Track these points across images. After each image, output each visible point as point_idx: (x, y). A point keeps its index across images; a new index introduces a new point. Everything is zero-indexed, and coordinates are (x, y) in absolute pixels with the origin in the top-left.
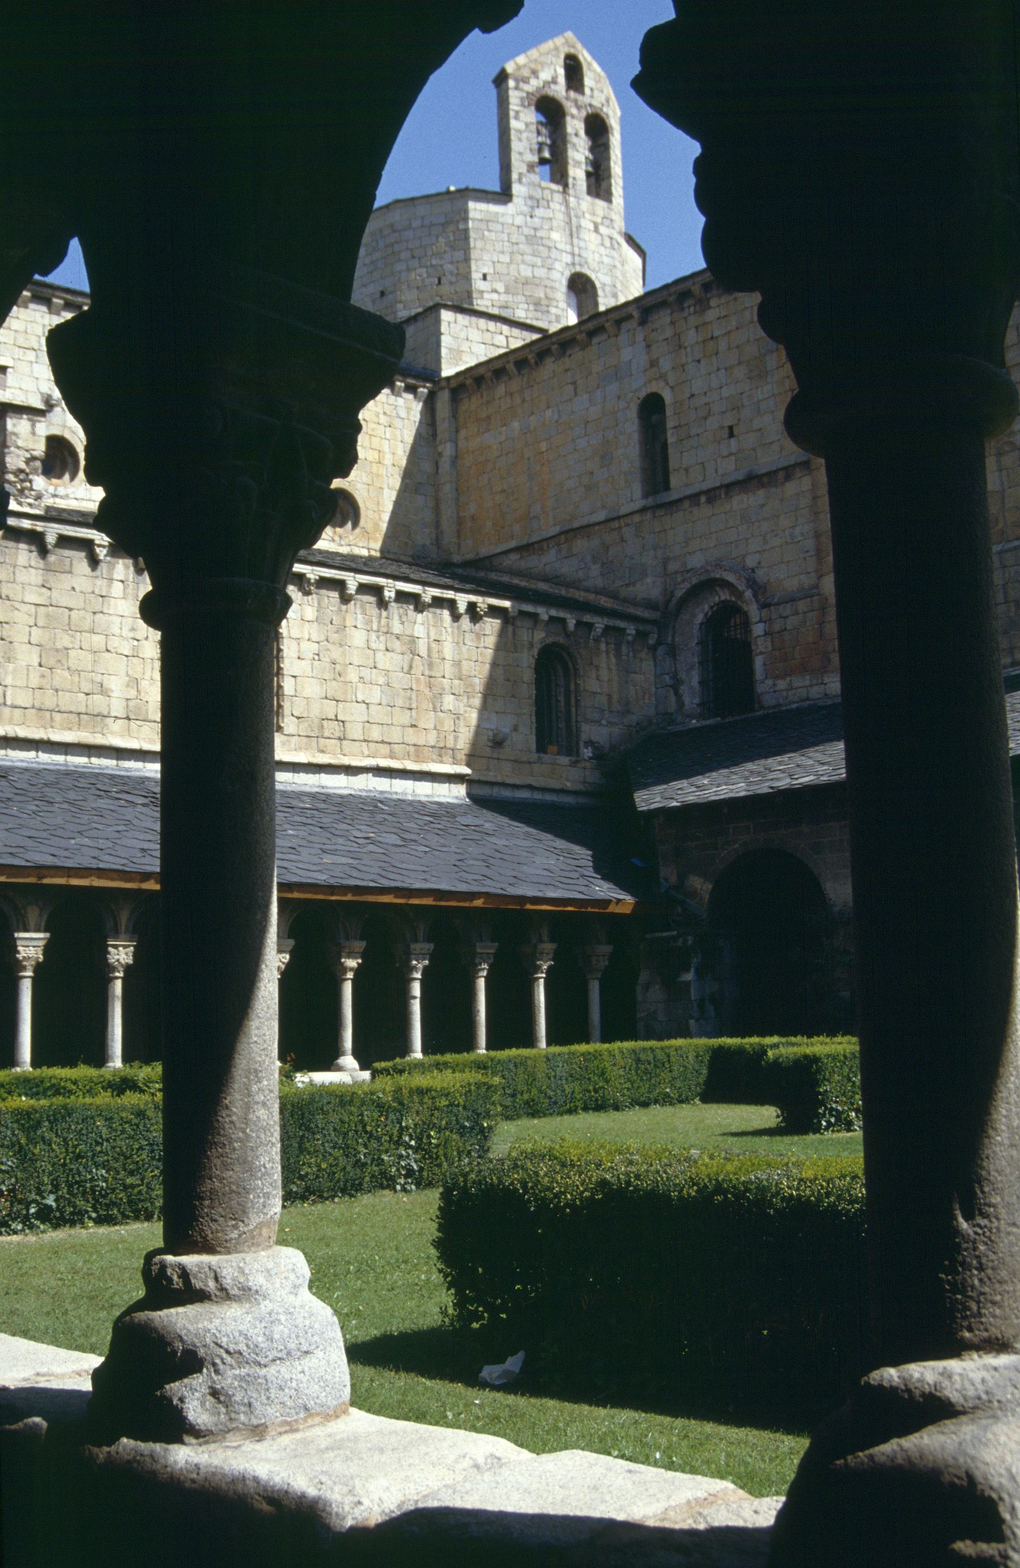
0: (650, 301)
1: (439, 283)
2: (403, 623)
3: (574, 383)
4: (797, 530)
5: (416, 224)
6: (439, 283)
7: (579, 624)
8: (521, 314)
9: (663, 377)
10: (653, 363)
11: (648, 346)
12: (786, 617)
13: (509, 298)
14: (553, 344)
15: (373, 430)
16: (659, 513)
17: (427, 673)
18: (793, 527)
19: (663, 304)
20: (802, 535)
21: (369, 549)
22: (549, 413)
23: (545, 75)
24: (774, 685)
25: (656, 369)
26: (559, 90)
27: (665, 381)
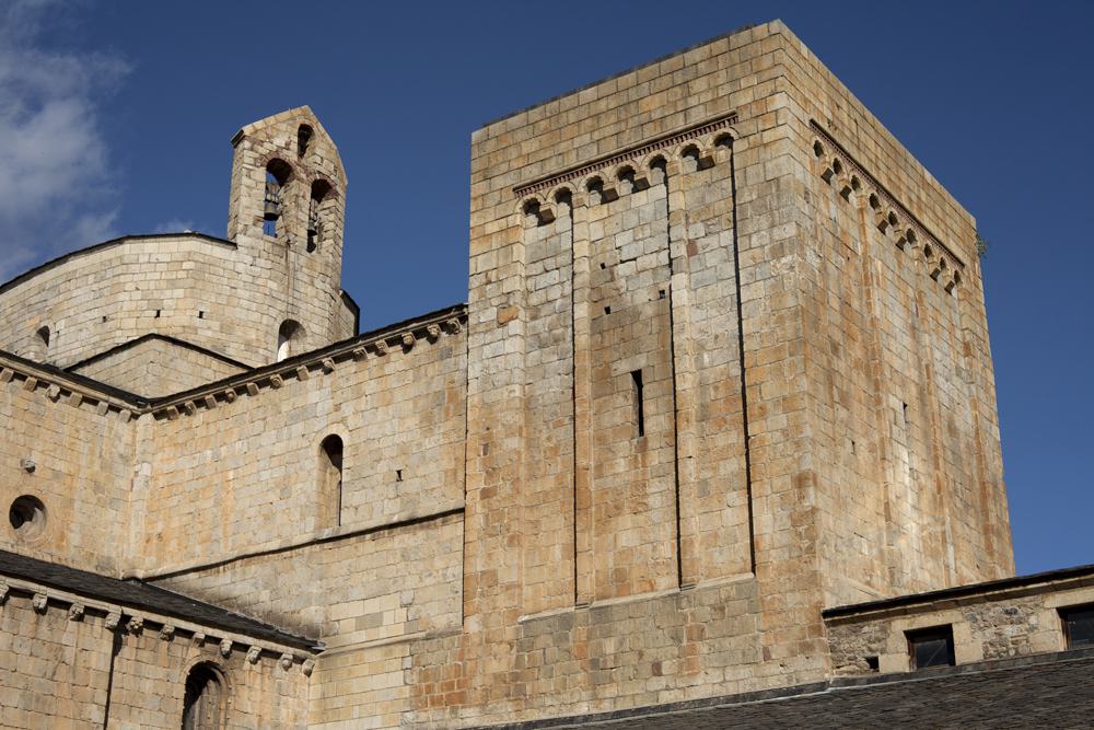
1: (158, 315)
2: (51, 630)
5: (146, 259)
6: (158, 315)
7: (236, 646)
8: (232, 352)
9: (343, 421)
10: (337, 407)
12: (433, 652)
13: (224, 337)
14: (250, 381)
16: (326, 546)
17: (71, 681)
20: (454, 576)
23: (280, 141)
24: (417, 717)
25: (338, 413)
26: (291, 156)
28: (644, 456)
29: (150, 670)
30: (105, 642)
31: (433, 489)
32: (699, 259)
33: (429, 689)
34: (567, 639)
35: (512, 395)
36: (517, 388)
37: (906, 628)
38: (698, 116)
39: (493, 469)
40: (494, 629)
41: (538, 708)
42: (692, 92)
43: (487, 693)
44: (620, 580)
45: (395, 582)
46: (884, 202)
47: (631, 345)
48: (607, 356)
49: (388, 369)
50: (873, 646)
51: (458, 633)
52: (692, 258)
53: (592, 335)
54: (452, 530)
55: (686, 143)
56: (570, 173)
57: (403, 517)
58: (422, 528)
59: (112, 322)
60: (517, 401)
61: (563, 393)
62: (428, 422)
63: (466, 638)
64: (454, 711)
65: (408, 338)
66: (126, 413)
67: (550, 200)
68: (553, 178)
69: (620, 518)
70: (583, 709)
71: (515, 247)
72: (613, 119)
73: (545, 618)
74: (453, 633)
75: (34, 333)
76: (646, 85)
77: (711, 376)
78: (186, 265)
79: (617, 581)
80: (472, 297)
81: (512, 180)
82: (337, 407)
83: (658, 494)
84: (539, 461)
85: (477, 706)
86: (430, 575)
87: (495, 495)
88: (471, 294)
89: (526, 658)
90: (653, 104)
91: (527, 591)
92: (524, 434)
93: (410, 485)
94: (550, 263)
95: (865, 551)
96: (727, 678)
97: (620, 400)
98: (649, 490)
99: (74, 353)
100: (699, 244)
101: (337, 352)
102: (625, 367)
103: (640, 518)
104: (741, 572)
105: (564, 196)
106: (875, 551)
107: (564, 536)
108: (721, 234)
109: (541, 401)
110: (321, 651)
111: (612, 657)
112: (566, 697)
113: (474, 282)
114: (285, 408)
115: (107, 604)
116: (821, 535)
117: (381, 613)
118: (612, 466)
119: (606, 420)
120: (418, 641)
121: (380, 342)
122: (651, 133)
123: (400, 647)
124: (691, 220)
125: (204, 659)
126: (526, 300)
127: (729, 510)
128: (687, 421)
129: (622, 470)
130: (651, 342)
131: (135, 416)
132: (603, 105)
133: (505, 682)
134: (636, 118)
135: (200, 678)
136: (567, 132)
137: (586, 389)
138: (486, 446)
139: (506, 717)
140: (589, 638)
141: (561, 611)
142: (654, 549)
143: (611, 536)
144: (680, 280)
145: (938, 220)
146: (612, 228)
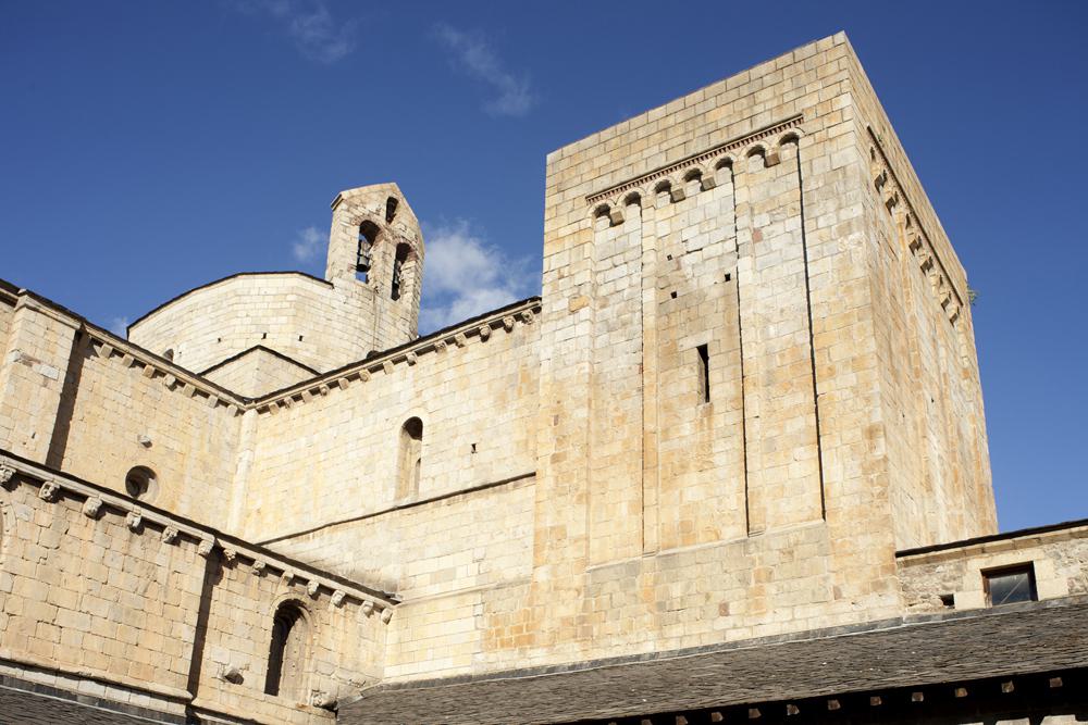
4: (520, 529)
10: (419, 394)
18: (518, 526)
28: (709, 420)
29: (240, 601)
30: (197, 567)
31: (505, 459)
32: (765, 245)
33: (499, 633)
34: (634, 584)
35: (582, 372)
36: (587, 365)
38: (764, 121)
39: (564, 437)
40: (562, 577)
41: (605, 648)
42: (758, 101)
43: (555, 636)
44: (686, 530)
45: (468, 541)
47: (696, 322)
48: (674, 334)
49: (467, 358)
51: (528, 582)
52: (758, 244)
53: (658, 317)
54: (526, 491)
55: (753, 144)
56: (640, 180)
57: (477, 485)
58: (495, 492)
60: (587, 376)
61: (630, 368)
62: (502, 402)
63: (536, 585)
64: (522, 651)
65: (485, 330)
67: (619, 204)
68: (623, 186)
69: (686, 476)
70: (649, 648)
71: (586, 245)
72: (681, 130)
73: (612, 566)
74: (522, 583)
76: (713, 100)
77: (777, 346)
79: (683, 532)
80: (545, 292)
81: (586, 190)
82: (419, 394)
83: (725, 454)
84: (607, 429)
85: (545, 646)
86: (501, 533)
87: (565, 458)
88: (544, 288)
89: (594, 603)
90: (720, 116)
91: (594, 544)
92: (593, 406)
93: (484, 455)
94: (618, 260)
95: (915, 513)
97: (686, 372)
98: (714, 450)
100: (764, 231)
101: (421, 345)
103: (706, 475)
105: (634, 199)
106: (921, 515)
107: (631, 494)
108: (787, 221)
109: (609, 377)
110: (398, 602)
111: (679, 600)
112: (633, 638)
113: (547, 279)
115: (201, 532)
117: (454, 569)
118: (678, 430)
119: (673, 390)
120: (488, 591)
121: (459, 334)
122: (716, 140)
123: (472, 596)
124: (756, 212)
125: (293, 596)
126: (596, 292)
128: (755, 384)
129: (687, 433)
130: (717, 320)
132: (671, 121)
133: (572, 625)
134: (703, 129)
135: (288, 615)
136: (637, 146)
137: (652, 364)
138: (557, 417)
139: (572, 657)
140: (656, 583)
141: (626, 560)
142: (720, 502)
143: (677, 493)
144: (745, 263)
146: (678, 224)
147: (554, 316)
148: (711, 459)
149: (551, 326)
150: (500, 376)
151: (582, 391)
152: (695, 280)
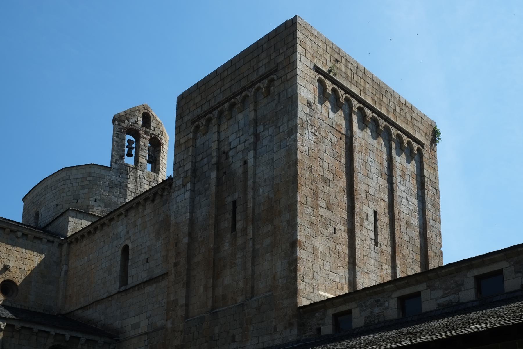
0: (127, 207)
1: (78, 202)
3: (104, 241)
5: (72, 177)
9: (129, 238)
10: (128, 232)
11: (127, 226)
14: (98, 225)
15: (30, 258)
19: (131, 208)
21: (21, 305)
22: (96, 253)
27: (130, 240)
31: (159, 265)
36: (188, 214)
37: (333, 313)
46: (368, 112)
49: (146, 212)
50: (320, 322)
59: (59, 206)
60: (188, 220)
61: (207, 215)
66: (56, 244)
75: (35, 214)
78: (89, 179)
82: (128, 232)
96: (260, 341)
99: (47, 221)
102: (229, 200)
104: (269, 292)
114: (111, 235)
116: (302, 271)
127: (266, 263)
131: (60, 245)
138: (176, 244)
145: (407, 121)
147: (176, 189)
148: (235, 262)
149: (176, 193)
150: (157, 222)
151: (186, 229)
152: (233, 164)
